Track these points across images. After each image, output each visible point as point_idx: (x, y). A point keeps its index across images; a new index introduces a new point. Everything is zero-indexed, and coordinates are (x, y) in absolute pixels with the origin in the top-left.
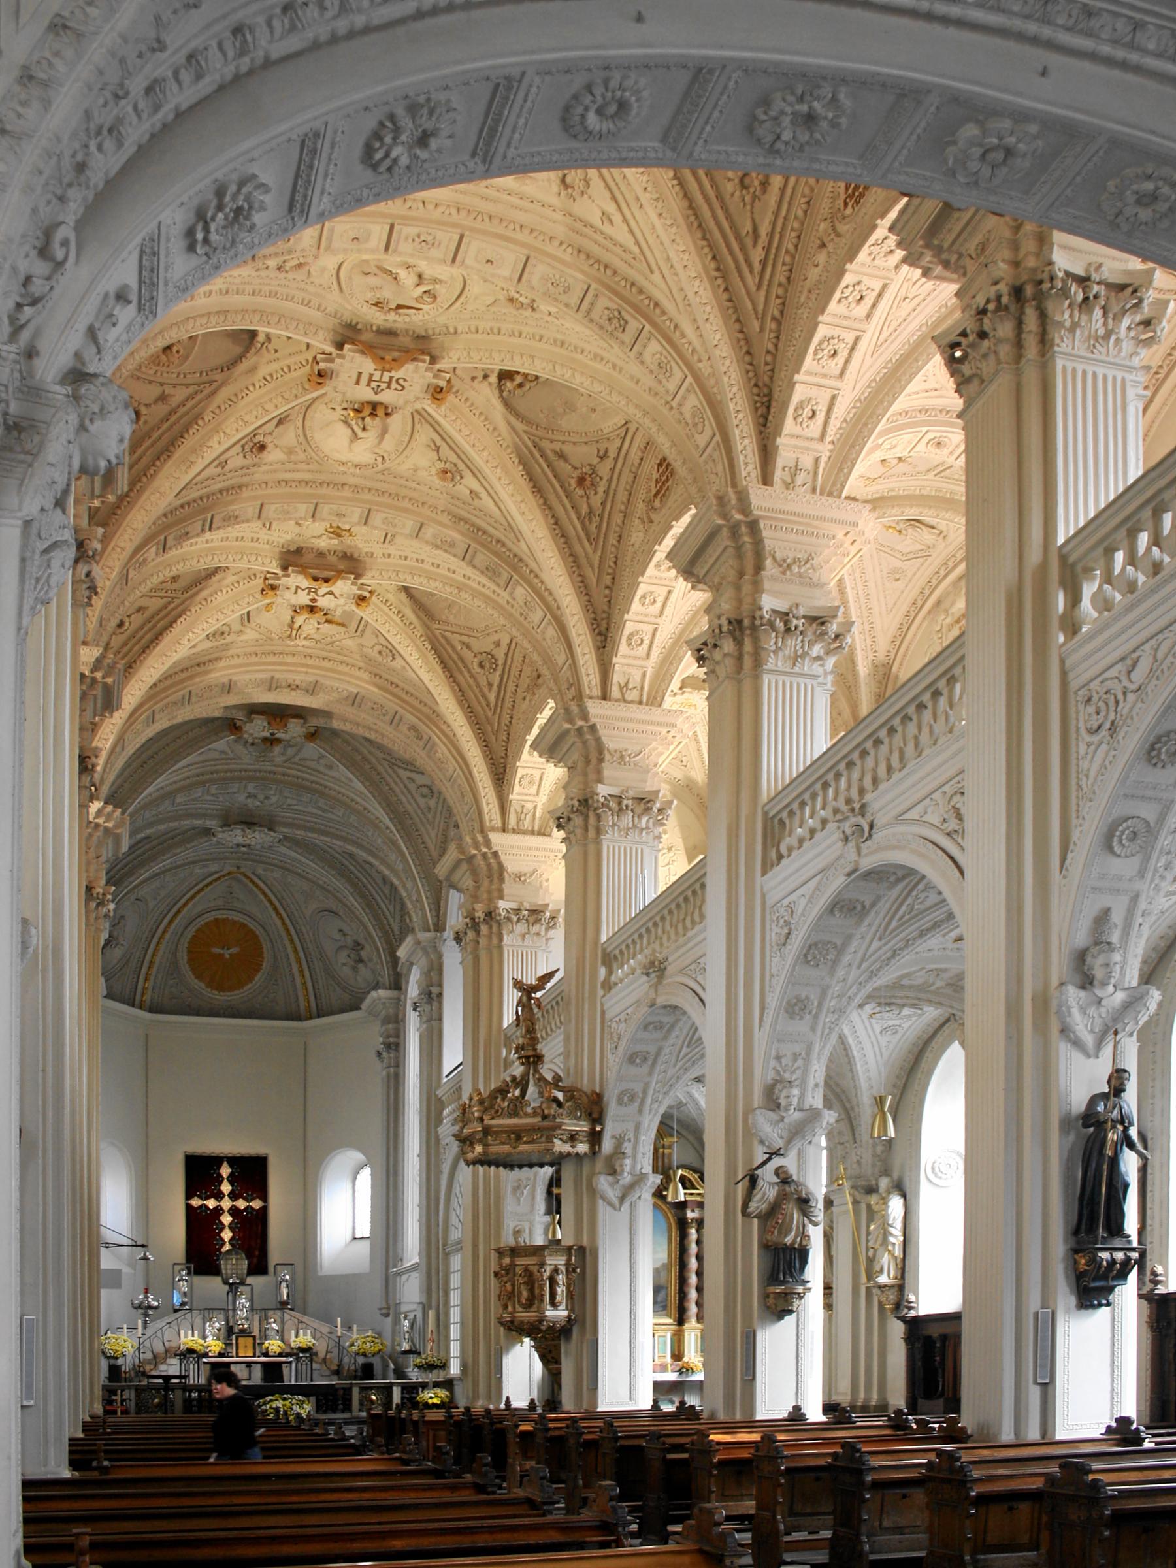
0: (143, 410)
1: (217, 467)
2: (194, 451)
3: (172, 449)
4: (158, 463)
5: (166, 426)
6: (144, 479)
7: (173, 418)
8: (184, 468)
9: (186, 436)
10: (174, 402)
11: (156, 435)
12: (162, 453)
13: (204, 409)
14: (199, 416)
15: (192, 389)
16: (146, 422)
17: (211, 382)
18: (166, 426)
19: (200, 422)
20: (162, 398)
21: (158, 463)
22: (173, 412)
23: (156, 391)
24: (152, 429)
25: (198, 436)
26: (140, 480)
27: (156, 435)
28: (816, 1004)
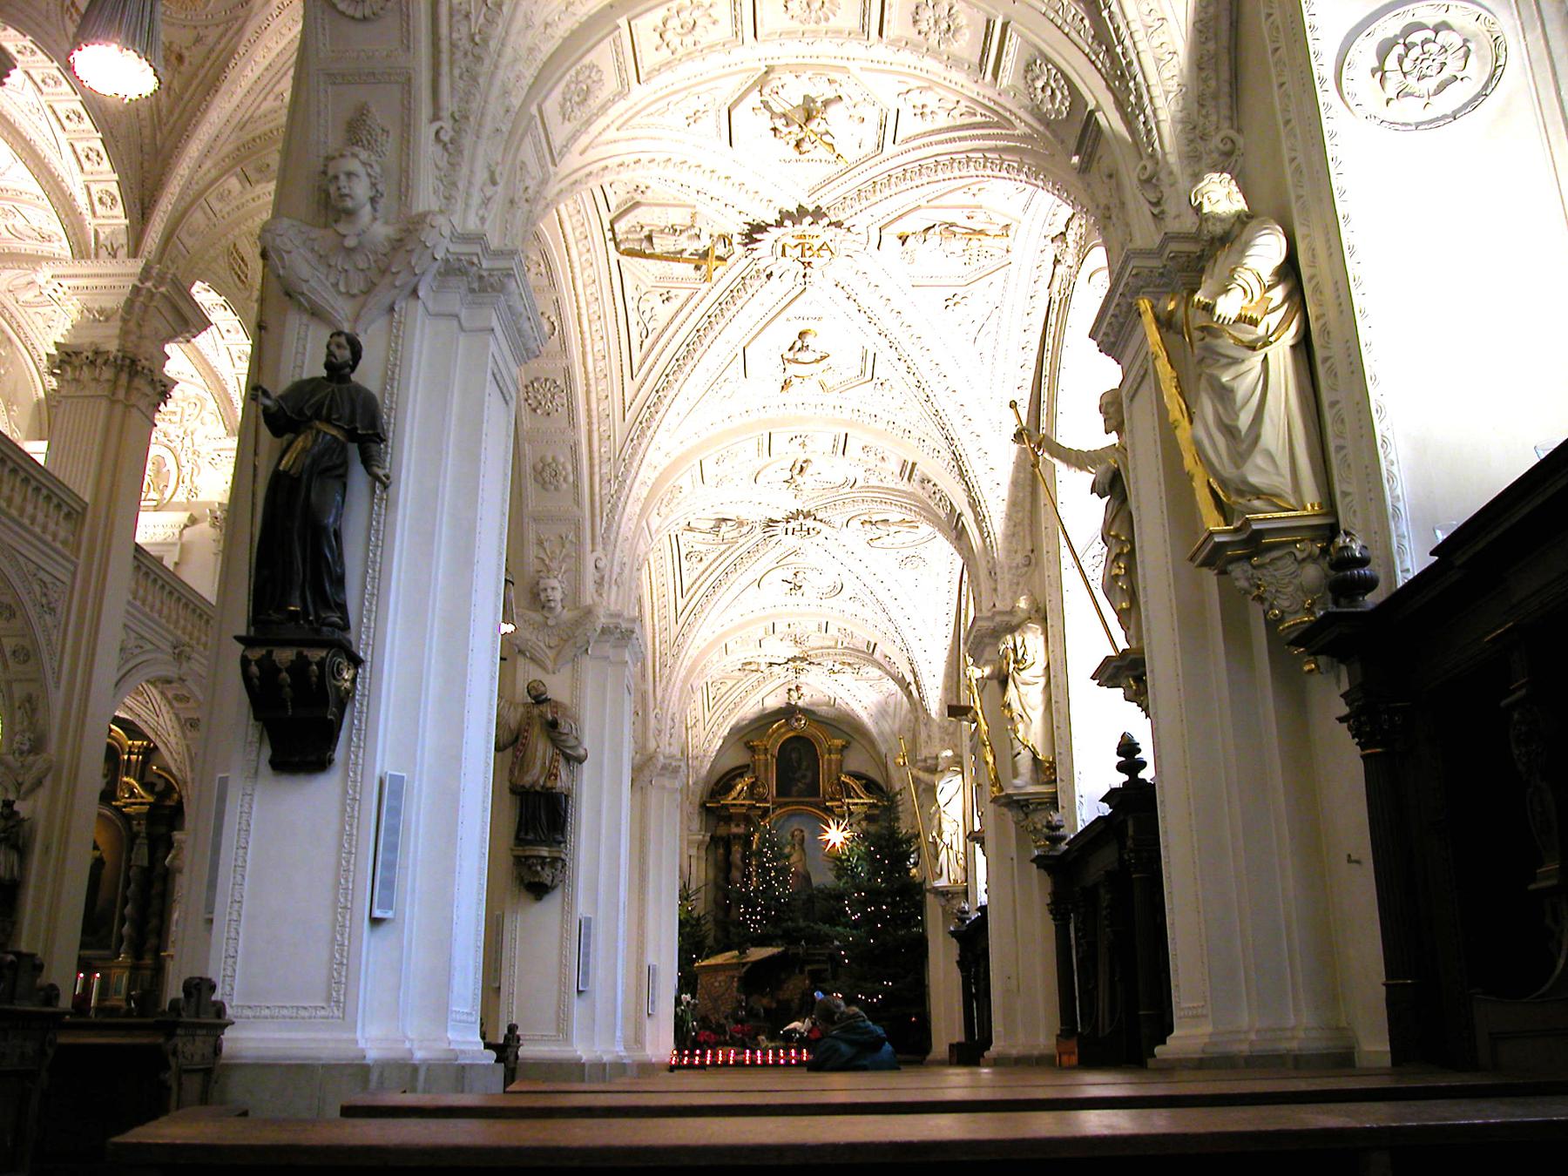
0: (186, 53)
1: (275, 100)
2: (234, 82)
3: (218, 84)
4: (208, 98)
5: (208, 64)
6: (199, 114)
7: (213, 57)
8: (227, 99)
9: (227, 70)
10: (210, 40)
11: (201, 75)
12: (210, 88)
13: (238, 43)
14: (233, 52)
15: (222, 28)
16: (190, 63)
17: (236, 19)
18: (208, 64)
19: (236, 56)
20: (198, 40)
21: (208, 98)
22: (211, 50)
23: (190, 35)
24: (198, 69)
25: (237, 69)
26: (195, 116)
27: (201, 75)
28: (569, 468)
